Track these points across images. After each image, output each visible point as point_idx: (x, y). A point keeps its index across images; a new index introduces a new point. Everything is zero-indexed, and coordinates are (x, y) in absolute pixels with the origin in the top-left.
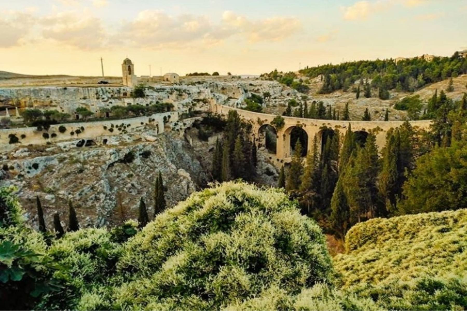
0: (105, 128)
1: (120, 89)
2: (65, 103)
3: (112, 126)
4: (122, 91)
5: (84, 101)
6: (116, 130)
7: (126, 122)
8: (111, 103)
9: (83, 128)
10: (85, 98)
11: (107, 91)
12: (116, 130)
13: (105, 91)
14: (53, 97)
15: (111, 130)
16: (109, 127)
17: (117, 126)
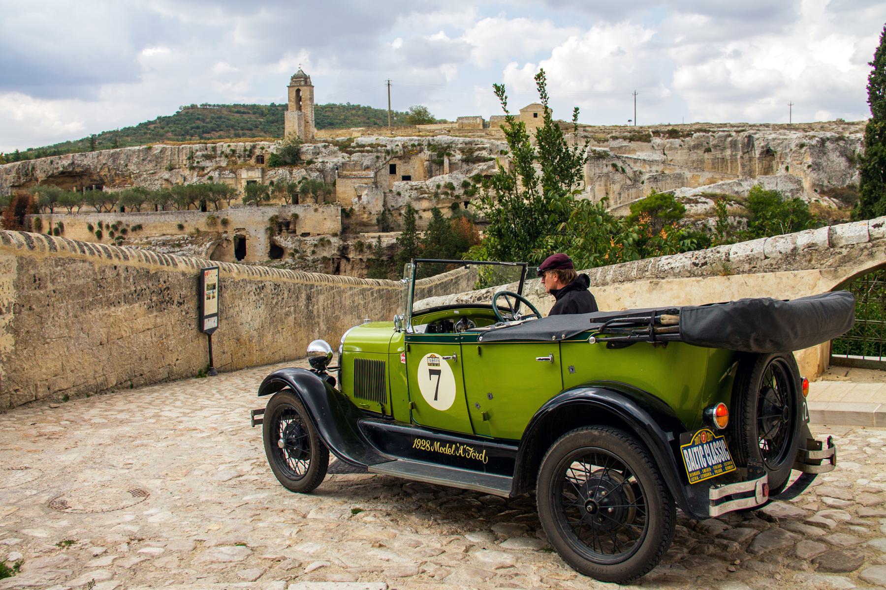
0: (91, 228)
1: (254, 147)
2: (142, 178)
3: (100, 225)
4: (258, 152)
5: (166, 175)
6: (106, 234)
7: (130, 219)
8: (211, 178)
9: (61, 225)
10: (171, 168)
11: (223, 152)
12: (106, 234)
13: (219, 152)
14: (132, 167)
15: (100, 235)
16: (96, 229)
17: (108, 227)
